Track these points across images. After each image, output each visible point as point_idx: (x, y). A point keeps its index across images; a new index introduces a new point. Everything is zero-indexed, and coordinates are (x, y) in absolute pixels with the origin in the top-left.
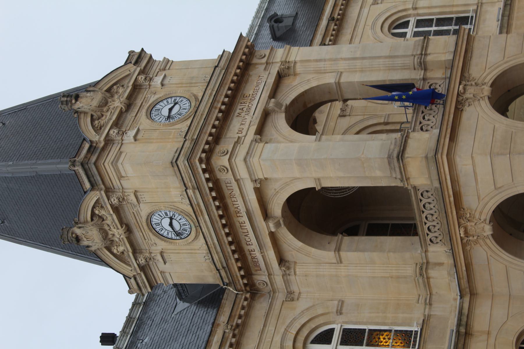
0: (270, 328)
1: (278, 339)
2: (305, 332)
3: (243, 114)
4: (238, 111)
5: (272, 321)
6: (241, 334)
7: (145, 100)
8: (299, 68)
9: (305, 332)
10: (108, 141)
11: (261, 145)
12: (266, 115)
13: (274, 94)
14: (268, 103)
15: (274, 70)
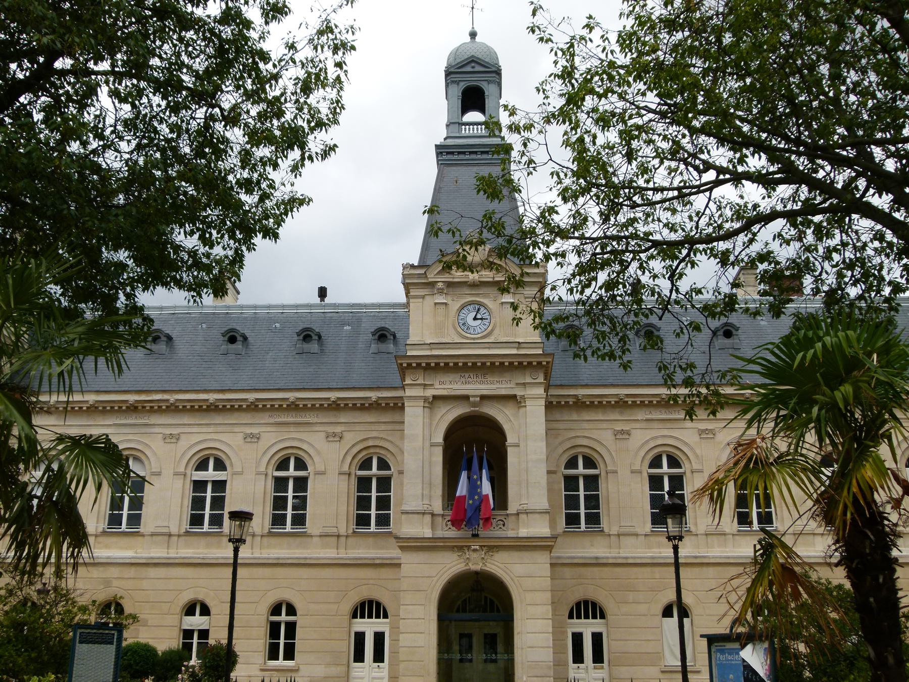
0: (383, 427)
1: (374, 434)
2: (382, 452)
3: (463, 380)
4: (467, 375)
5: (390, 427)
6: (376, 409)
7: (485, 296)
8: (522, 410)
9: (382, 452)
10: (432, 285)
11: (422, 404)
12: (466, 398)
13: (483, 398)
14: (473, 396)
15: (519, 392)
